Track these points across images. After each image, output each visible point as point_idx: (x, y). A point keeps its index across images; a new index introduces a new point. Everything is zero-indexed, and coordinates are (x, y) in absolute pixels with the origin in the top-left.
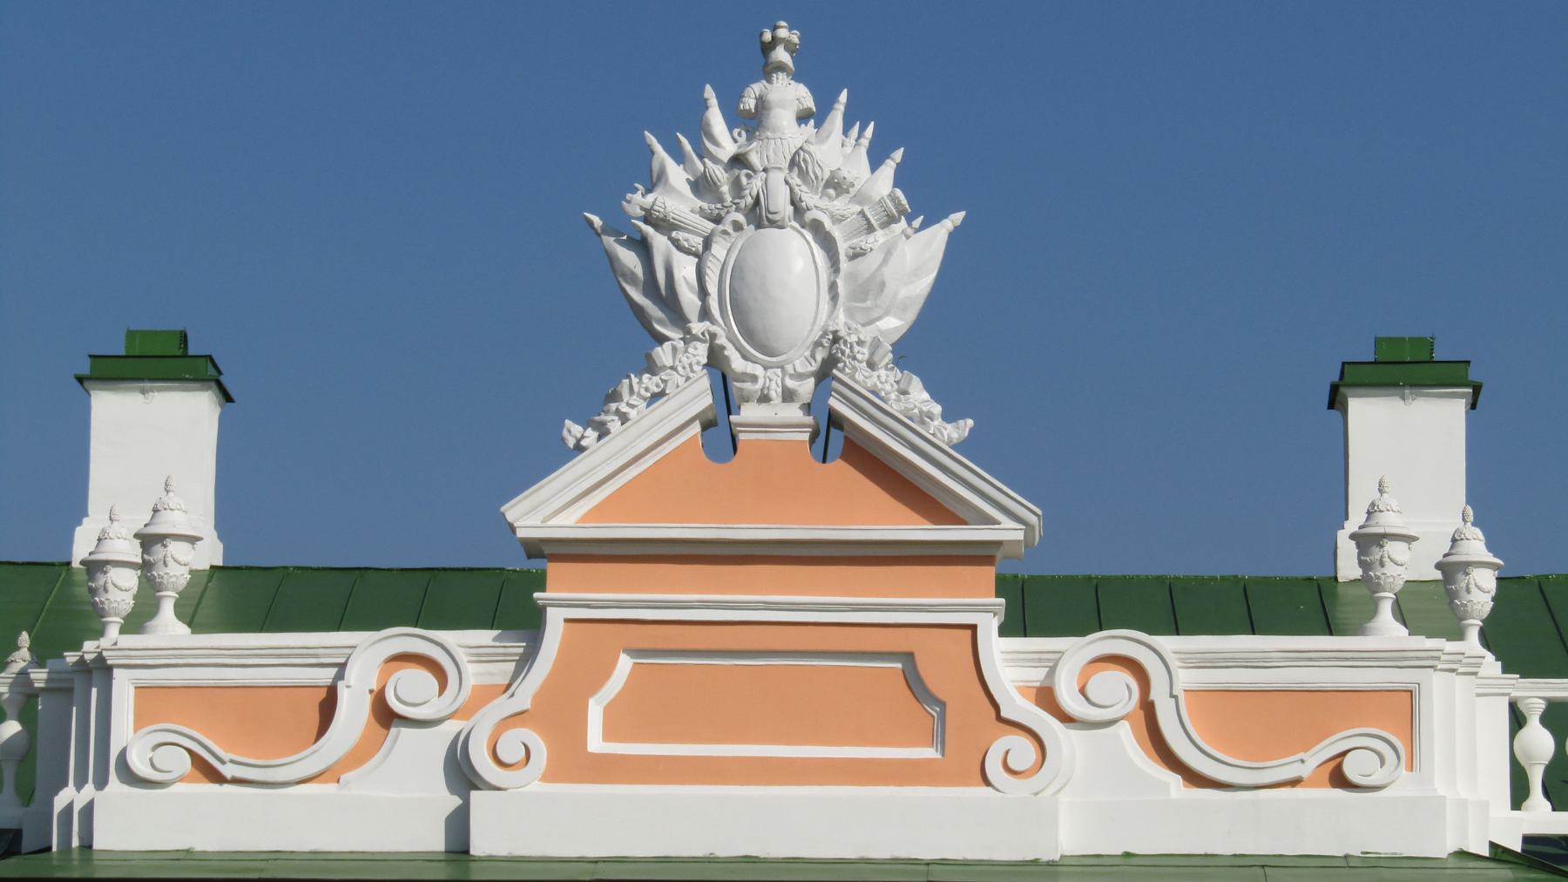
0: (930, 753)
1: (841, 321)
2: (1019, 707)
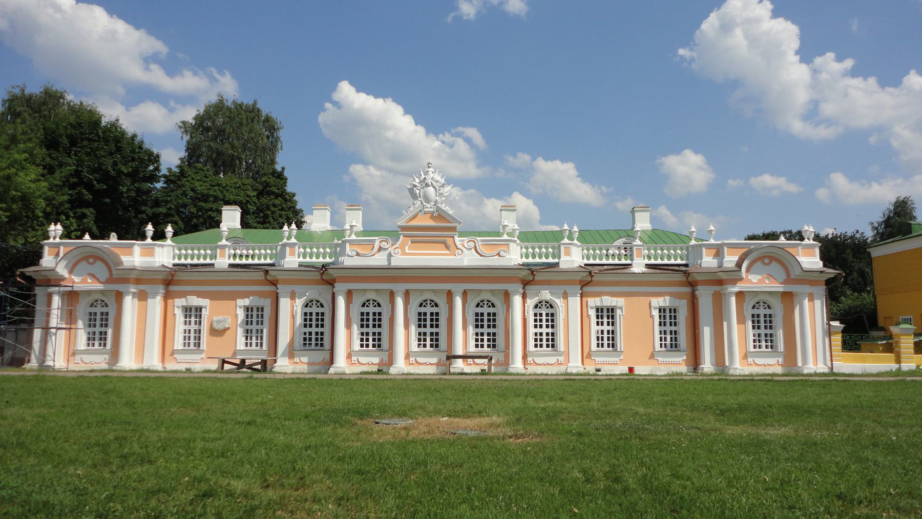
0: (448, 252)
1: (437, 199)
2: (459, 246)
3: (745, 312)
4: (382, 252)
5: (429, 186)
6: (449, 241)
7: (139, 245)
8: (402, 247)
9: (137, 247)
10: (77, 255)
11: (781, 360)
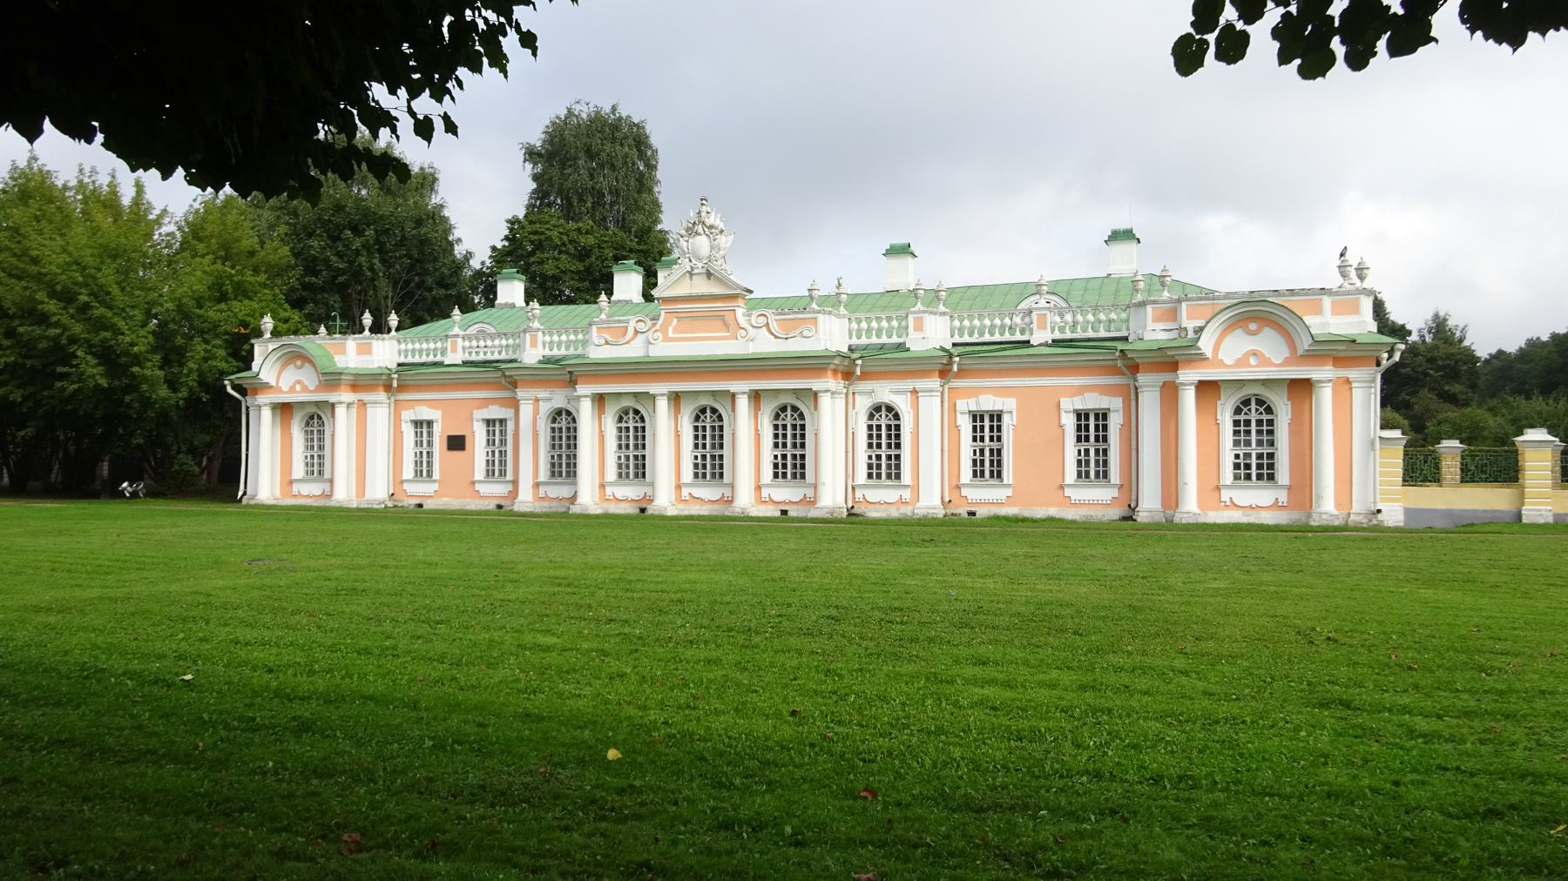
3: (1219, 417)
4: (639, 336)
5: (700, 234)
6: (729, 317)
7: (354, 339)
8: (664, 330)
9: (351, 342)
10: (282, 356)
11: (1283, 496)
